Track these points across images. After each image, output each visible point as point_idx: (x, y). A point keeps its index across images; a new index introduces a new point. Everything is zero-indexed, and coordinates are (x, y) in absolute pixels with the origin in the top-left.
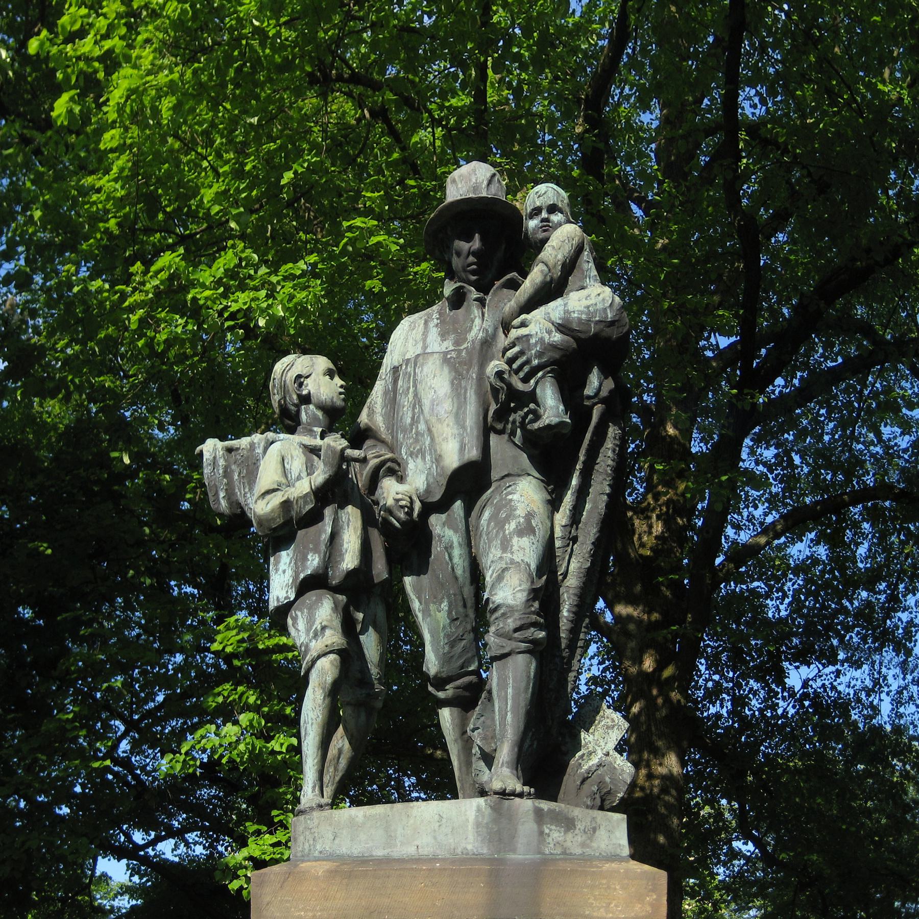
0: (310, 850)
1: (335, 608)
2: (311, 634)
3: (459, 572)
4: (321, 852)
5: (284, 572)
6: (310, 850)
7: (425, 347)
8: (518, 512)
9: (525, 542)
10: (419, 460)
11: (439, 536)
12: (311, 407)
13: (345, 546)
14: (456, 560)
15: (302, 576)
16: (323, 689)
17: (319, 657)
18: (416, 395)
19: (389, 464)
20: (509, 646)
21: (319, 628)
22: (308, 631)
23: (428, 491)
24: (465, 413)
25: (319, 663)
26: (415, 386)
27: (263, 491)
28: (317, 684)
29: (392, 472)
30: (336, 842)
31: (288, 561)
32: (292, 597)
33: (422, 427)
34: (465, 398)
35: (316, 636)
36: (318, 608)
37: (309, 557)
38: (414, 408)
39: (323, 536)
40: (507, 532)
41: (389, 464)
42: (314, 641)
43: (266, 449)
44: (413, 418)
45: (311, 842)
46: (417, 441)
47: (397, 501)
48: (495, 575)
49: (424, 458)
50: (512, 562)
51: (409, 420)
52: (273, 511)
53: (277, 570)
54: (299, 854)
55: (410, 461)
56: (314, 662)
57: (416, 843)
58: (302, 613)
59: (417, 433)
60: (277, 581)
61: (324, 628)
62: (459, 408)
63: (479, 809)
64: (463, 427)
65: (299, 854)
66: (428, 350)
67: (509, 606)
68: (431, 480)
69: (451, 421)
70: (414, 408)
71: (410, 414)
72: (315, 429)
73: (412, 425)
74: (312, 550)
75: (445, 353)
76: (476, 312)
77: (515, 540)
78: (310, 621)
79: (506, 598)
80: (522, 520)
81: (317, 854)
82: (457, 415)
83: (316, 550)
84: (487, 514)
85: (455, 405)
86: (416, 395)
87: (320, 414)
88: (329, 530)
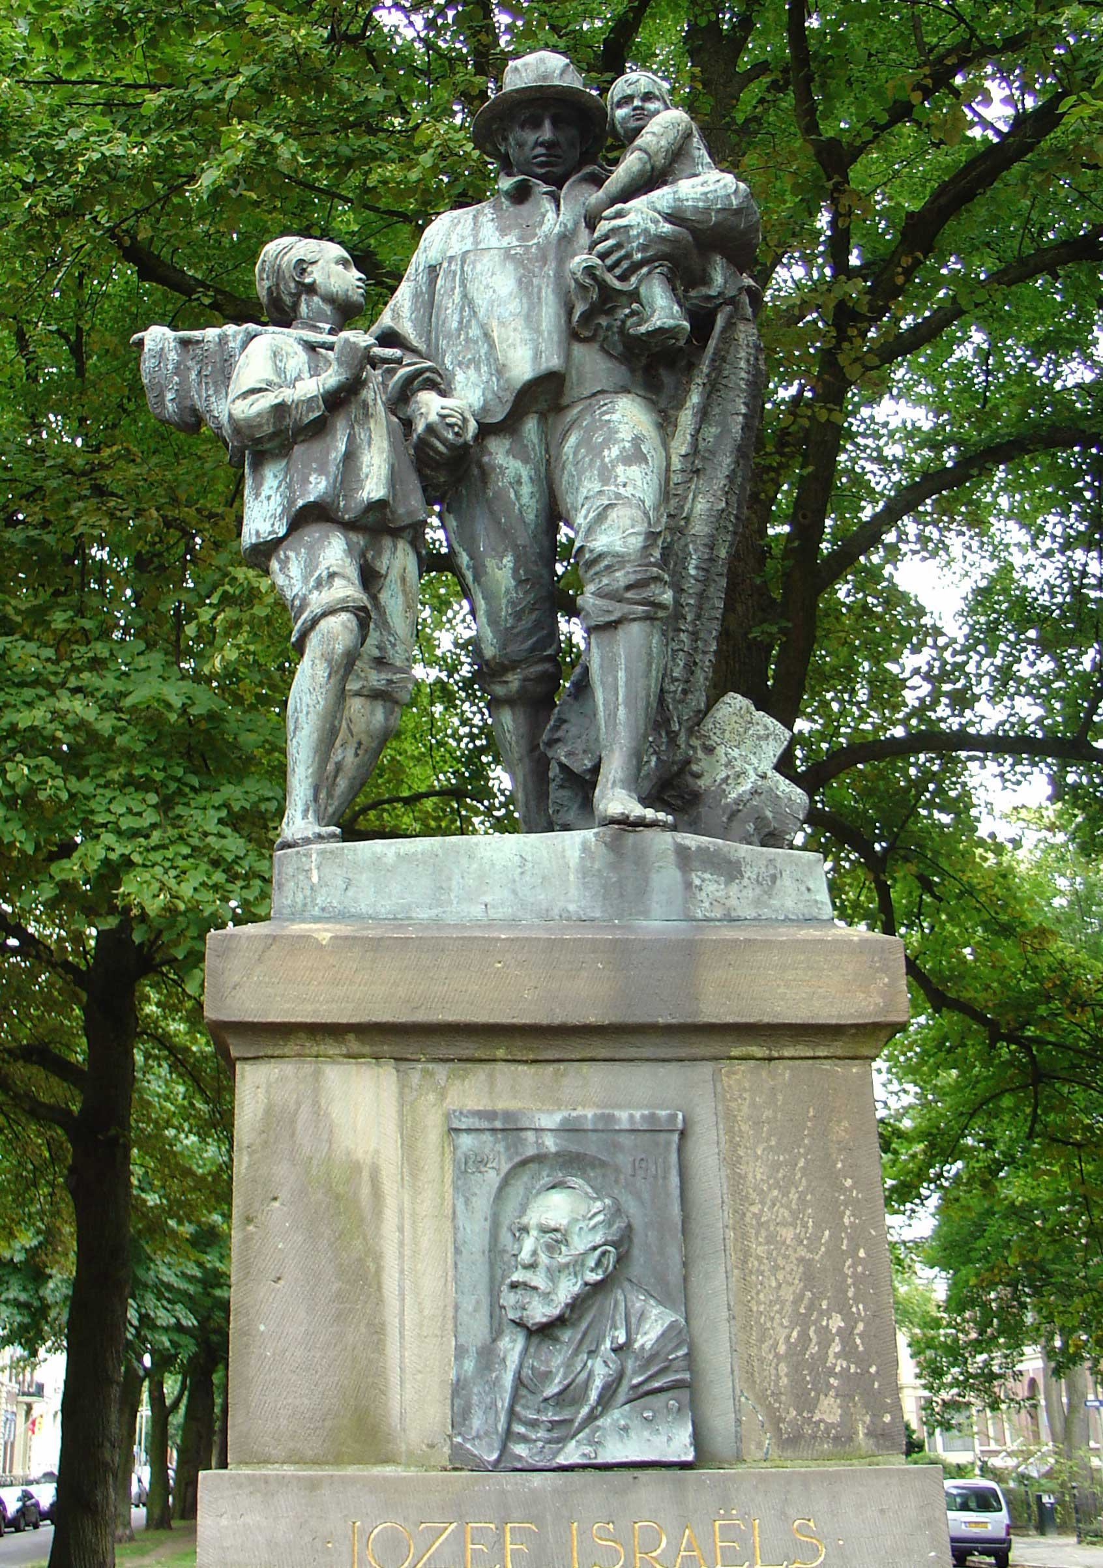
0: (305, 905)
1: (350, 551)
2: (312, 583)
3: (530, 516)
4: (323, 909)
5: (269, 498)
6: (305, 905)
7: (476, 243)
8: (620, 436)
9: (635, 472)
10: (472, 372)
11: (501, 467)
12: (316, 299)
13: (365, 470)
14: (525, 500)
15: (300, 503)
16: (329, 662)
17: (325, 614)
18: (465, 296)
19: (428, 374)
20: (618, 610)
21: (325, 574)
22: (305, 580)
23: (485, 409)
24: (539, 314)
25: (323, 624)
26: (463, 285)
27: (245, 389)
28: (319, 654)
29: (432, 385)
30: (350, 893)
31: (275, 484)
32: (282, 532)
33: (475, 332)
34: (539, 298)
35: (319, 585)
36: (323, 548)
37: (312, 479)
38: (462, 310)
39: (333, 455)
40: (607, 460)
41: (428, 374)
42: (316, 593)
43: (245, 345)
44: (460, 322)
45: (308, 892)
46: (466, 347)
47: (443, 417)
48: (592, 515)
49: (478, 369)
50: (618, 496)
51: (455, 325)
52: (259, 415)
53: (257, 495)
54: (287, 911)
55: (458, 371)
56: (315, 622)
57: (488, 899)
58: (298, 554)
59: (467, 340)
60: (256, 510)
61: (332, 576)
62: (530, 310)
63: (585, 848)
64: (538, 331)
65: (287, 911)
66: (481, 246)
67: (616, 555)
68: (490, 396)
69: (520, 323)
70: (462, 310)
71: (456, 317)
72: (321, 325)
73: (459, 330)
74: (316, 470)
75: (508, 249)
76: (548, 205)
77: (620, 469)
78: (311, 565)
79: (611, 544)
80: (627, 445)
81: (316, 911)
82: (528, 318)
83: (322, 471)
84: (572, 440)
85: (525, 306)
86: (465, 296)
87: (327, 309)
88: (342, 447)
